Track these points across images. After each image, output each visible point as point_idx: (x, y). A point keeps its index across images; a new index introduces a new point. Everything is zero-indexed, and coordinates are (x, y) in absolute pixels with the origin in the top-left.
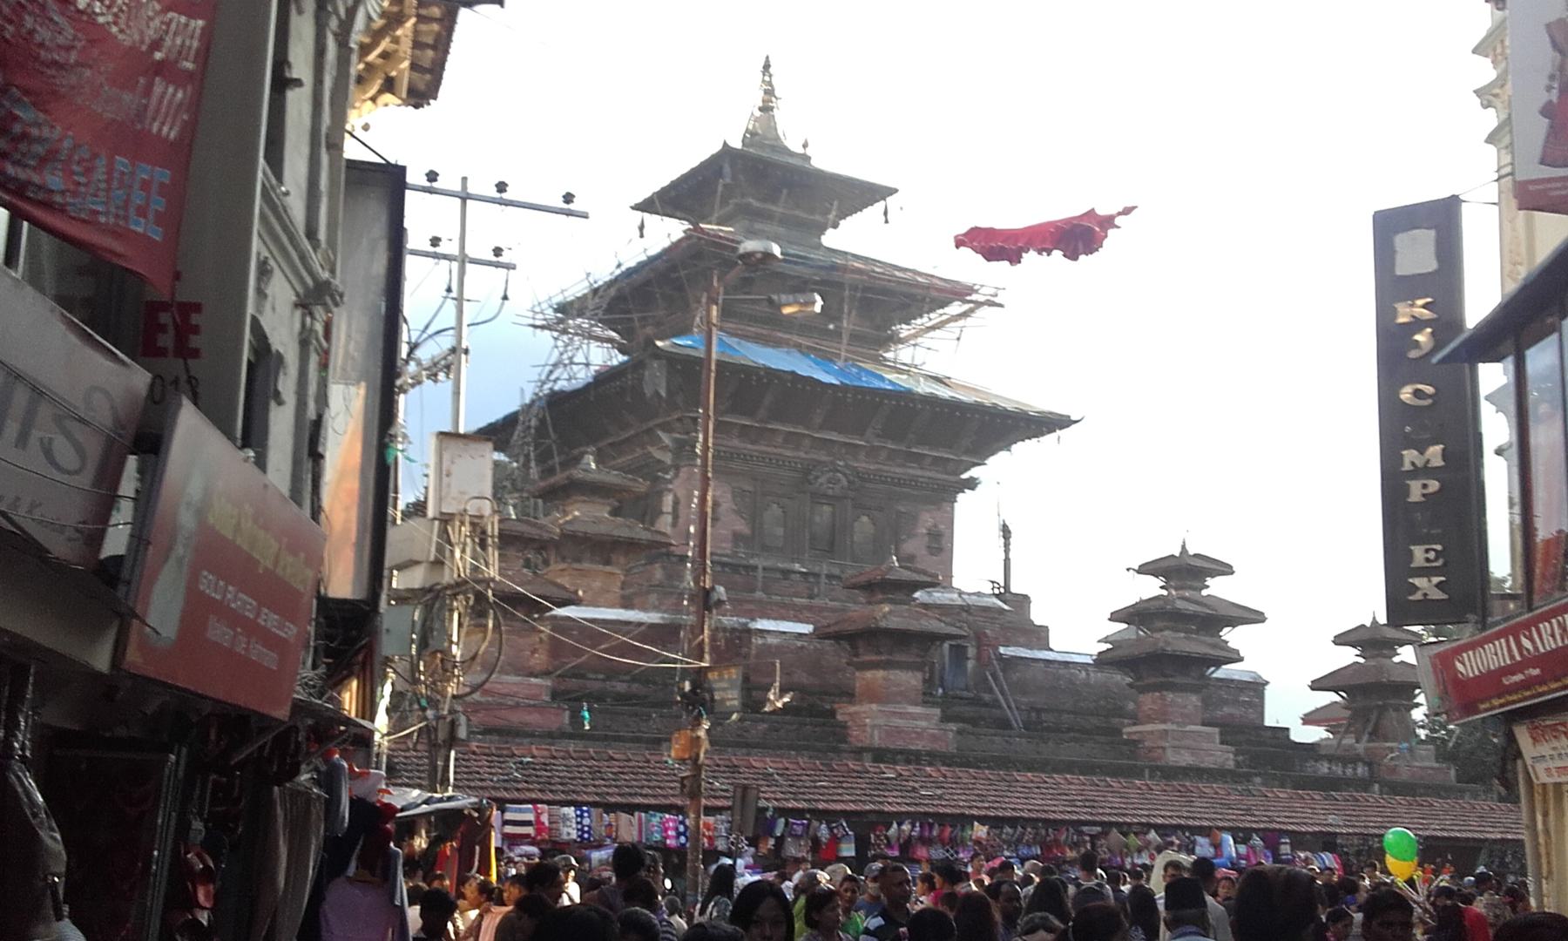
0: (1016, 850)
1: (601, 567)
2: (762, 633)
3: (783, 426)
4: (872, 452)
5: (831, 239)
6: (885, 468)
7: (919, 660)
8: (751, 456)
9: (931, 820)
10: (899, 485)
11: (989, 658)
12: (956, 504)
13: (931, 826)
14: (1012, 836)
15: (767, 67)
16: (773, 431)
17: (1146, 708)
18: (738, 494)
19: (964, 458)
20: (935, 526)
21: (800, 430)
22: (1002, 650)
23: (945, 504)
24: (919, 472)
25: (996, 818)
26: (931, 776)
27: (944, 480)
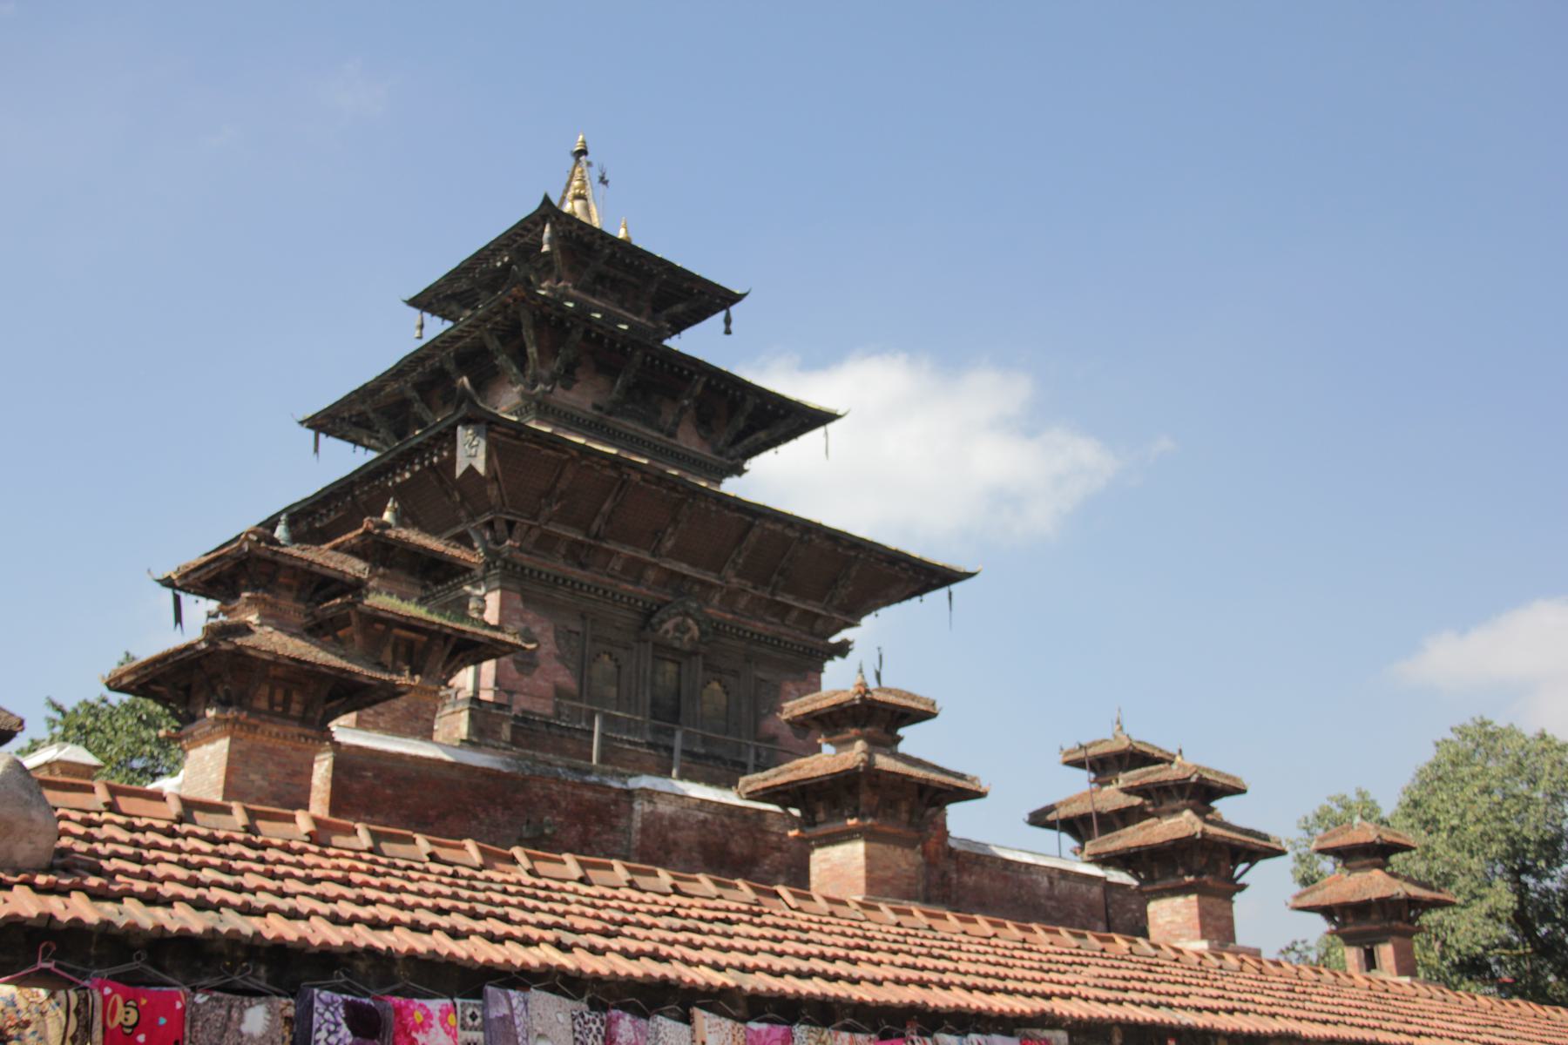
2: (650, 795)
5: (667, 343)
16: (610, 553)
17: (1160, 921)
18: (563, 635)
19: (835, 615)
21: (645, 556)
23: (811, 674)
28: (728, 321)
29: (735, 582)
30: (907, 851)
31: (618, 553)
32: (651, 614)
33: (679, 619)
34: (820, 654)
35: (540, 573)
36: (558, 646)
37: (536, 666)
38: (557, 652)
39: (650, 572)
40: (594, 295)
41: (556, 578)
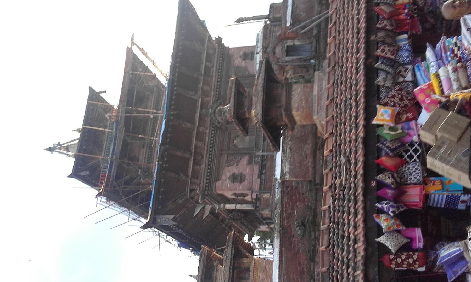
0: (404, 64)
1: (251, 273)
2: (283, 175)
3: (193, 141)
4: (205, 94)
6: (213, 88)
7: (285, 88)
8: (210, 158)
9: (374, 184)
10: (221, 78)
11: (293, 32)
12: (230, 47)
13: (381, 185)
14: (388, 73)
15: (51, 150)
19: (206, 45)
20: (241, 57)
22: (288, 25)
23: (230, 53)
24: (215, 68)
25: (367, 94)
26: (331, 151)
27: (218, 55)
28: (102, 92)
29: (200, 93)
30: (293, 89)
31: (195, 145)
32: (215, 126)
33: (216, 115)
34: (222, 50)
35: (207, 176)
36: (234, 164)
37: (241, 174)
38: (235, 165)
39: (201, 129)
40: (103, 145)
41: (208, 169)
